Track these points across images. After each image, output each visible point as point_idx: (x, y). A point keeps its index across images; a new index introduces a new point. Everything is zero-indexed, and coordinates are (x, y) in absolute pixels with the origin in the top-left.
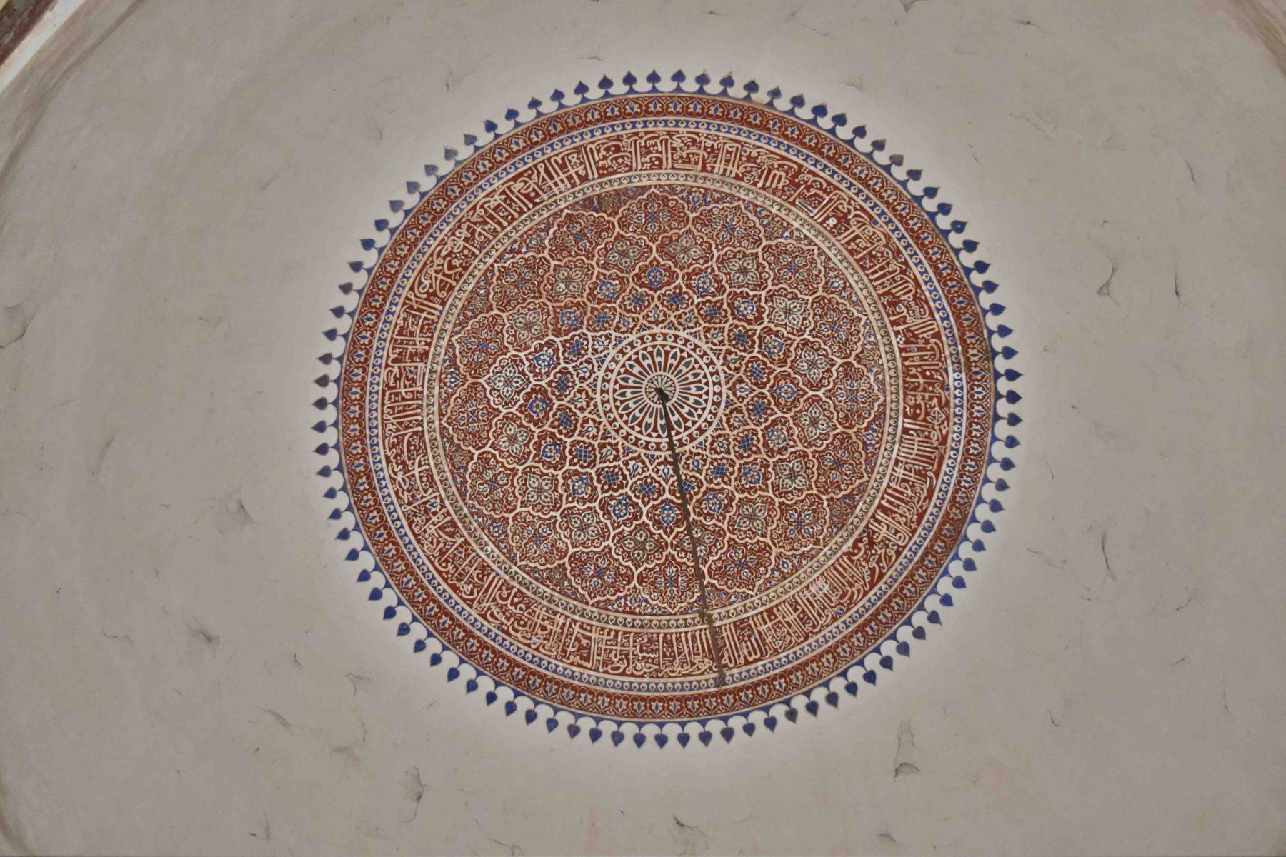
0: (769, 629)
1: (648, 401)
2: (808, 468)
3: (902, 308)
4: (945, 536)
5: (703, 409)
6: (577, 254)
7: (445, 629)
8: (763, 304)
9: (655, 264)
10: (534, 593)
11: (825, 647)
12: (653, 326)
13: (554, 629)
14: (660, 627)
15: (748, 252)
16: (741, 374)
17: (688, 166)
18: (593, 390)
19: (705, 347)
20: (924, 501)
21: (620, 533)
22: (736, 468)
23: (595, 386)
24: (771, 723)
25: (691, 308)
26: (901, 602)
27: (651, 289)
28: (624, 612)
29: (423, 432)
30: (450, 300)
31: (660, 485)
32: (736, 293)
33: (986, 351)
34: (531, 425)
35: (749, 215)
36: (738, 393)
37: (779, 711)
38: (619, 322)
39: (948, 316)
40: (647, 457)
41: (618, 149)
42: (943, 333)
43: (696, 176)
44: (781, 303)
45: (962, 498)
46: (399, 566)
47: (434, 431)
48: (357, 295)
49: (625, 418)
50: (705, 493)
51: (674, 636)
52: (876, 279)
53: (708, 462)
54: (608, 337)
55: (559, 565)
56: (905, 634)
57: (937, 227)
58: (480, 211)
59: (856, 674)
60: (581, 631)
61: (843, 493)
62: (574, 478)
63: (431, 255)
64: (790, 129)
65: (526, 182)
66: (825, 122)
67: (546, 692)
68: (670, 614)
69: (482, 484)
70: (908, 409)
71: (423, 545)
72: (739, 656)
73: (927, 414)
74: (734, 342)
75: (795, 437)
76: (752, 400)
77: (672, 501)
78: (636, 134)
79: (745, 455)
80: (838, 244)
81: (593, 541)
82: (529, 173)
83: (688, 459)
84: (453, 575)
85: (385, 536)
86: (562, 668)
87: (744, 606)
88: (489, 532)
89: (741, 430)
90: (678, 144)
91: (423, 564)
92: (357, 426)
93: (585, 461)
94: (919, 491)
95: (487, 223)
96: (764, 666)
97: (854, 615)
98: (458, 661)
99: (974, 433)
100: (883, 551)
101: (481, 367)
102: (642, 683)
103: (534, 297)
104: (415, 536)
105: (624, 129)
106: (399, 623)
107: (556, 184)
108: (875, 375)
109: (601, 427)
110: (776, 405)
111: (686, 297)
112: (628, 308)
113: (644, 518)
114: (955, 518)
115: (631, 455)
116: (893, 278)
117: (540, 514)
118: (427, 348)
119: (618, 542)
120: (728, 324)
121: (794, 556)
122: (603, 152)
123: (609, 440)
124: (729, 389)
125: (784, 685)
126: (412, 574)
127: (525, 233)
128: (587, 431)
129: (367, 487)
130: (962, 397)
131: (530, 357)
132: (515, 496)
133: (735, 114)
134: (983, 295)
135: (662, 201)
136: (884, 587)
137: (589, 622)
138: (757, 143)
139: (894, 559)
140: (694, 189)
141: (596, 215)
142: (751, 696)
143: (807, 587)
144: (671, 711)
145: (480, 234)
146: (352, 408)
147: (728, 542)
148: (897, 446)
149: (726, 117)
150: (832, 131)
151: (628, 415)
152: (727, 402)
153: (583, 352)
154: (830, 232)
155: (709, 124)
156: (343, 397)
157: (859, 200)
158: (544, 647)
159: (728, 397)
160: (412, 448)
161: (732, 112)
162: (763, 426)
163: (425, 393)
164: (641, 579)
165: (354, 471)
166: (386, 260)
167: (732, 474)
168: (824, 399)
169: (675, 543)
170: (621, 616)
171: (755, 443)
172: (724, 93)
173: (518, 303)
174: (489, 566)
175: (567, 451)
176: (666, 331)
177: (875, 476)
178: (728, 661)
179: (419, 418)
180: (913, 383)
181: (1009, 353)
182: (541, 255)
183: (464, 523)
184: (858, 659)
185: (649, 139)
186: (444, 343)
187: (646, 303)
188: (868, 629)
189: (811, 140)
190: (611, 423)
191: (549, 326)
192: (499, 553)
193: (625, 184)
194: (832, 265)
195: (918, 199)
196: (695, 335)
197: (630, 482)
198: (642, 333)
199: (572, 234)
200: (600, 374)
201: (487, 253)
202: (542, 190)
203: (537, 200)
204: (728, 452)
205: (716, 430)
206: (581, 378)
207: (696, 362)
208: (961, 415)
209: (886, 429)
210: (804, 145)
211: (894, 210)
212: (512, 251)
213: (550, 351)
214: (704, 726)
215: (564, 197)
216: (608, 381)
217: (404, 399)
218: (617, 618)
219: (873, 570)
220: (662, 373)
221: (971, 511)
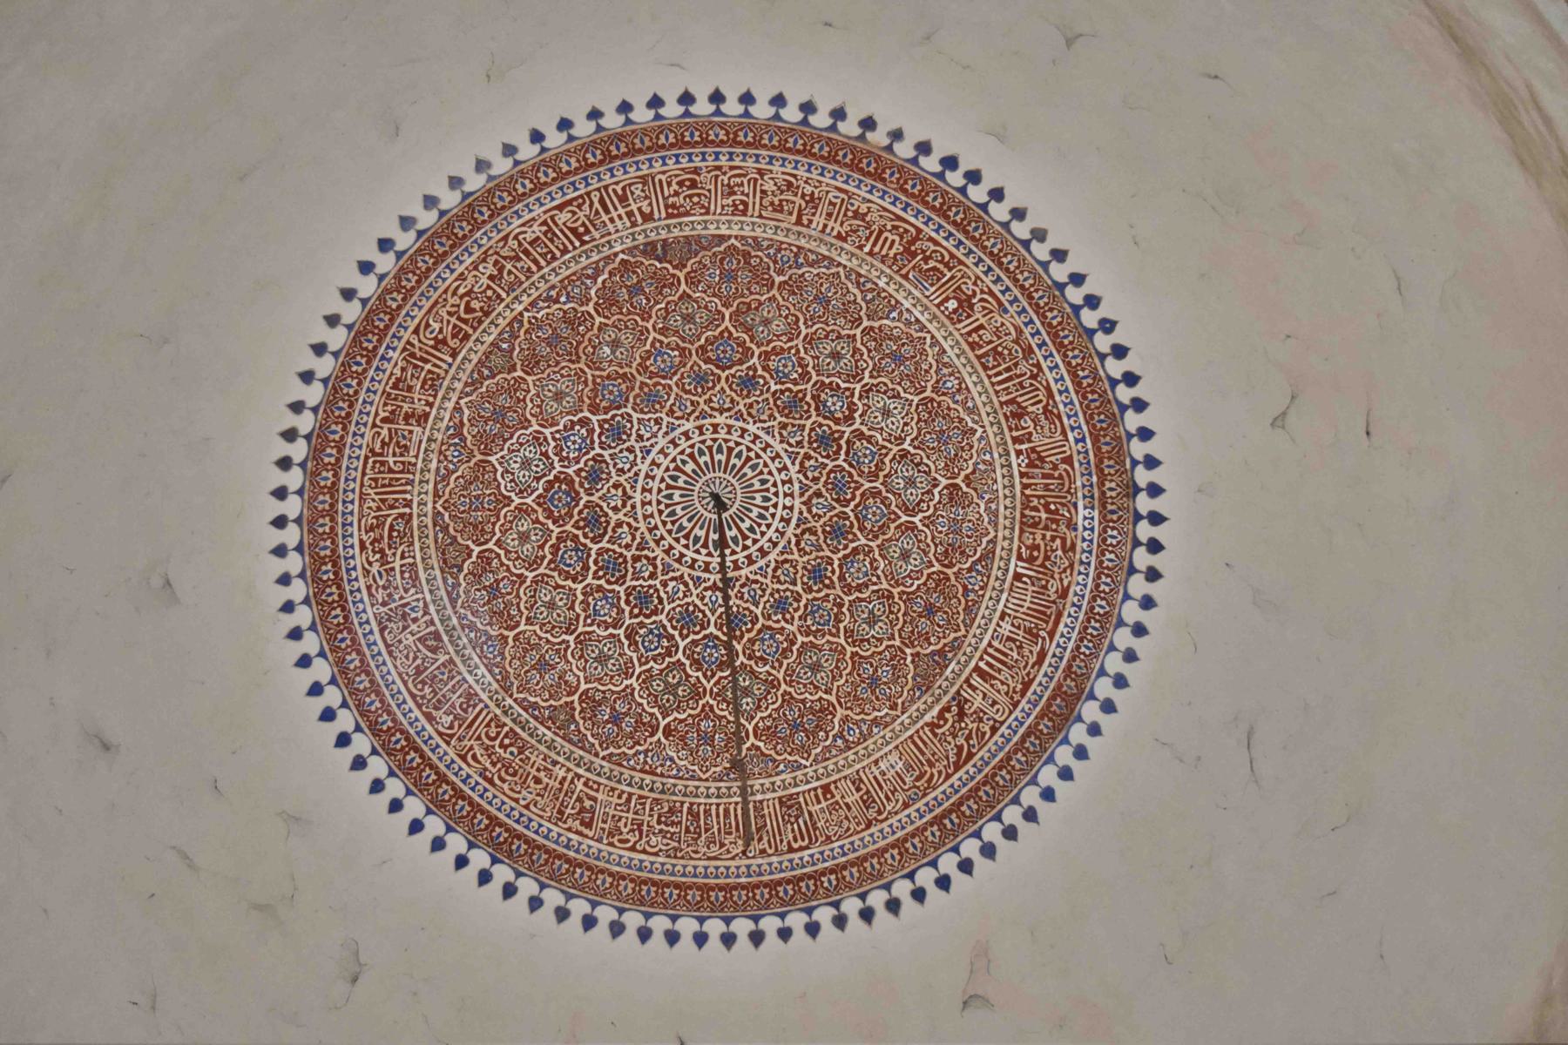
1: (700, 508)
3: (1027, 422)
5: (768, 526)
6: (629, 313)
7: (412, 768)
8: (855, 400)
10: (531, 735)
11: (891, 839)
13: (551, 783)
14: (685, 795)
15: (844, 333)
16: (820, 485)
18: (632, 487)
19: (778, 447)
20: (1033, 667)
22: (802, 604)
23: (636, 481)
24: (813, 929)
25: (765, 396)
26: (991, 792)
27: (718, 367)
28: (642, 771)
29: (411, 515)
30: (464, 352)
31: (705, 616)
32: (823, 382)
34: (550, 522)
35: (850, 285)
36: (814, 510)
38: (674, 404)
39: (1084, 437)
40: (692, 579)
41: (694, 185)
42: (1075, 457)
43: (788, 230)
44: (878, 401)
45: (1080, 667)
46: (361, 682)
47: (425, 515)
49: (669, 526)
50: (760, 631)
51: (702, 808)
52: (1000, 383)
53: (768, 592)
54: (658, 422)
55: (566, 703)
56: (992, 832)
57: (1081, 324)
58: (513, 243)
59: (926, 877)
61: (932, 648)
62: (596, 595)
63: (445, 292)
64: (910, 182)
65: (574, 213)
66: (955, 178)
67: (533, 862)
69: (479, 590)
70: (1023, 550)
71: (395, 658)
72: (782, 841)
73: (1047, 558)
74: (815, 445)
75: (879, 572)
76: (830, 520)
77: (717, 638)
78: (719, 168)
79: (815, 588)
80: (956, 333)
81: (612, 677)
82: (580, 201)
83: (743, 586)
84: (429, 701)
85: (348, 642)
86: (554, 834)
87: (795, 778)
88: (482, 651)
89: (813, 556)
91: (393, 682)
92: (327, 498)
93: (613, 576)
94: (1027, 653)
95: (519, 259)
96: (812, 856)
97: (932, 803)
98: (423, 810)
99: (1102, 587)
100: (975, 725)
101: (493, 441)
102: (655, 863)
103: (570, 361)
104: (387, 646)
105: (704, 160)
106: (354, 754)
107: (612, 220)
108: (986, 503)
109: (638, 535)
110: (859, 529)
111: (762, 381)
112: (687, 388)
113: (680, 655)
114: (1069, 692)
115: (671, 574)
116: (1020, 383)
117: (548, 636)
118: (427, 409)
119: (644, 682)
120: (810, 421)
122: (675, 187)
123: (646, 552)
125: (834, 883)
126: (378, 693)
127: (567, 277)
128: (620, 537)
129: (332, 577)
130: (1091, 541)
131: (558, 436)
132: (519, 610)
133: (845, 156)
134: (1130, 414)
135: (744, 256)
136: (972, 771)
138: (868, 196)
140: (784, 246)
141: (659, 266)
142: (791, 892)
143: (876, 762)
144: (688, 902)
145: (510, 272)
146: (324, 474)
147: (783, 695)
148: (1004, 596)
149: (831, 159)
150: (963, 190)
151: (673, 523)
152: (799, 519)
153: (624, 437)
154: (948, 317)
155: (810, 165)
157: (988, 280)
158: (535, 805)
159: (801, 513)
160: (395, 534)
161: (841, 153)
162: (840, 555)
163: (420, 465)
164: (668, 732)
165: (317, 554)
166: (387, 291)
167: (796, 610)
170: (638, 776)
171: (829, 574)
172: (833, 128)
173: (549, 366)
174: (476, 695)
175: (591, 561)
177: (974, 630)
178: (766, 846)
179: (408, 497)
180: (1033, 517)
181: (1155, 490)
182: (583, 309)
183: (451, 636)
184: (929, 858)
185: (735, 176)
186: (450, 405)
187: (710, 384)
188: (947, 822)
189: (935, 199)
190: (650, 530)
191: (586, 399)
192: (491, 680)
194: (946, 360)
195: (1061, 287)
196: (767, 431)
197: (668, 608)
199: (626, 286)
200: (644, 468)
201: (516, 298)
202: (594, 226)
203: (586, 238)
204: (795, 584)
205: (782, 553)
206: (618, 470)
207: (766, 465)
208: (1089, 564)
209: (994, 572)
210: (926, 203)
211: (1030, 297)
212: (548, 299)
213: (583, 431)
214: (728, 924)
215: (620, 237)
216: (653, 478)
217: (391, 471)
218: (632, 777)
219: (960, 748)
220: (721, 474)
221: (1089, 685)
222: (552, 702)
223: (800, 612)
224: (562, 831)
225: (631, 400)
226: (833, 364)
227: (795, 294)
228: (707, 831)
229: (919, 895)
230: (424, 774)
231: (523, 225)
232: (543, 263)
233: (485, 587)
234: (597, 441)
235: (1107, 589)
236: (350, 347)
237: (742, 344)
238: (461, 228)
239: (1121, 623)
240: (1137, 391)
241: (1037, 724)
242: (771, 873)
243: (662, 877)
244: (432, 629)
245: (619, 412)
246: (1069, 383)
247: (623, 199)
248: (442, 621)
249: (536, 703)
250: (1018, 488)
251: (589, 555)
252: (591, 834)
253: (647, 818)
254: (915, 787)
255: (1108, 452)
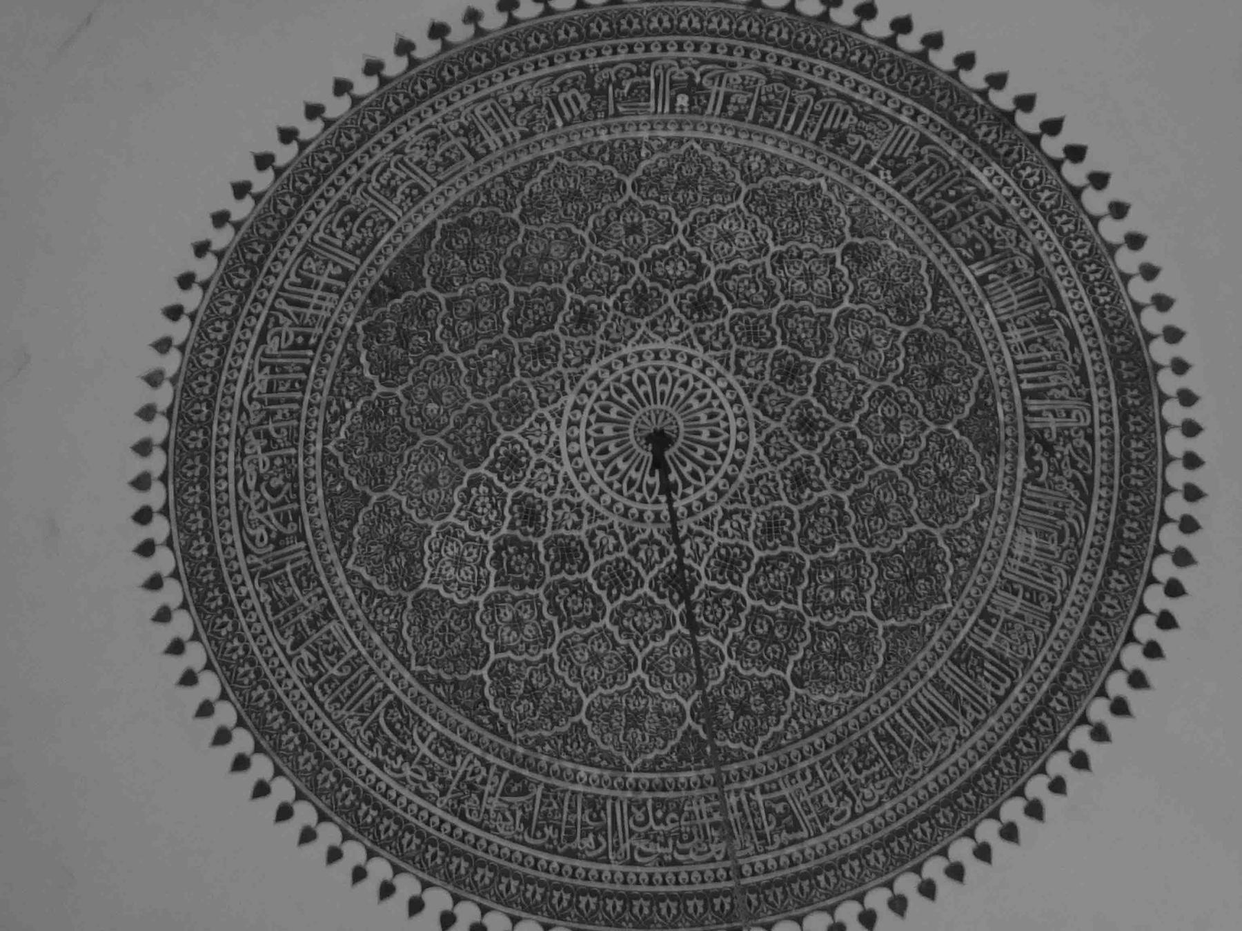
0: (998, 639)
2: (902, 404)
3: (854, 139)
4: (1130, 379)
5: (726, 419)
6: (418, 361)
7: (593, 913)
9: (524, 302)
10: (677, 789)
11: (1083, 617)
12: (585, 366)
14: (862, 726)
15: (619, 204)
16: (735, 346)
17: (456, 167)
19: (669, 345)
21: (735, 637)
22: (817, 462)
23: (571, 486)
24: (1081, 761)
28: (804, 736)
29: (396, 698)
31: (741, 547)
32: (648, 262)
33: (996, 118)
34: (528, 591)
35: (580, 164)
36: (751, 371)
37: (1080, 739)
41: (354, 216)
42: (927, 133)
43: (477, 171)
44: (711, 232)
46: (483, 877)
48: (184, 613)
49: (638, 496)
50: (802, 520)
51: (887, 726)
52: (796, 126)
53: (778, 478)
54: (540, 420)
55: (685, 733)
56: (1171, 537)
57: (809, 18)
59: (1146, 629)
60: (767, 797)
62: (628, 614)
63: (238, 497)
68: (864, 700)
69: (518, 704)
70: (964, 252)
77: (768, 558)
83: (751, 492)
85: (440, 854)
87: (949, 629)
88: (567, 753)
90: (419, 154)
91: (512, 852)
92: (307, 754)
94: (1056, 343)
95: (274, 413)
96: (1024, 690)
97: (1093, 552)
105: (337, 189)
107: (317, 307)
109: (617, 528)
111: (594, 306)
112: (536, 370)
113: (749, 602)
116: (813, 112)
117: (616, 687)
120: (671, 301)
121: (966, 524)
122: (340, 233)
124: (736, 373)
125: (1065, 700)
126: (507, 873)
127: (333, 384)
130: (1015, 194)
132: (570, 689)
133: (451, 72)
134: (933, 56)
136: (1104, 493)
137: (769, 778)
138: (510, 83)
139: (1089, 449)
141: (400, 301)
142: (1032, 741)
143: (1010, 554)
144: (944, 826)
145: (278, 431)
146: (285, 738)
147: (873, 560)
148: (987, 307)
149: (442, 85)
151: (640, 490)
152: (746, 391)
154: (690, 112)
155: (432, 106)
156: (263, 735)
157: (689, 53)
159: (742, 384)
162: (811, 391)
163: (364, 652)
164: (798, 681)
166: (185, 550)
167: (817, 472)
168: (856, 308)
169: (808, 606)
171: (817, 416)
173: (395, 467)
174: (597, 796)
175: (595, 588)
176: (605, 361)
177: (990, 361)
178: (974, 714)
179: (380, 685)
180: (944, 216)
182: (375, 394)
185: (380, 174)
186: (341, 578)
188: (1121, 559)
190: (625, 515)
193: (402, 243)
194: (729, 149)
196: (644, 340)
197: (702, 570)
198: (579, 386)
200: (567, 468)
201: (306, 443)
202: (307, 326)
204: (793, 450)
208: (1033, 217)
209: (958, 293)
211: (740, 35)
212: (335, 418)
213: (482, 488)
216: (584, 469)
217: (342, 680)
218: (801, 751)
219: (1074, 479)
222: (672, 743)
223: (823, 471)
224: (776, 854)
225: (498, 425)
226: (638, 239)
227: (540, 215)
228: (909, 744)
229: (1153, 650)
230: (609, 908)
231: (246, 384)
232: (298, 395)
233: (522, 698)
234: (502, 485)
235: (1071, 226)
236: (201, 620)
237: (544, 293)
238: (194, 439)
239: (1112, 249)
240: (920, 30)
241: (1124, 403)
242: (999, 737)
243: (902, 821)
244: (505, 776)
245: (498, 444)
246: (853, 75)
247: (307, 283)
248: (510, 762)
249: (657, 757)
250: (906, 202)
251: (590, 587)
252: (805, 834)
253: (844, 777)
254: (1064, 550)
255: (951, 104)
